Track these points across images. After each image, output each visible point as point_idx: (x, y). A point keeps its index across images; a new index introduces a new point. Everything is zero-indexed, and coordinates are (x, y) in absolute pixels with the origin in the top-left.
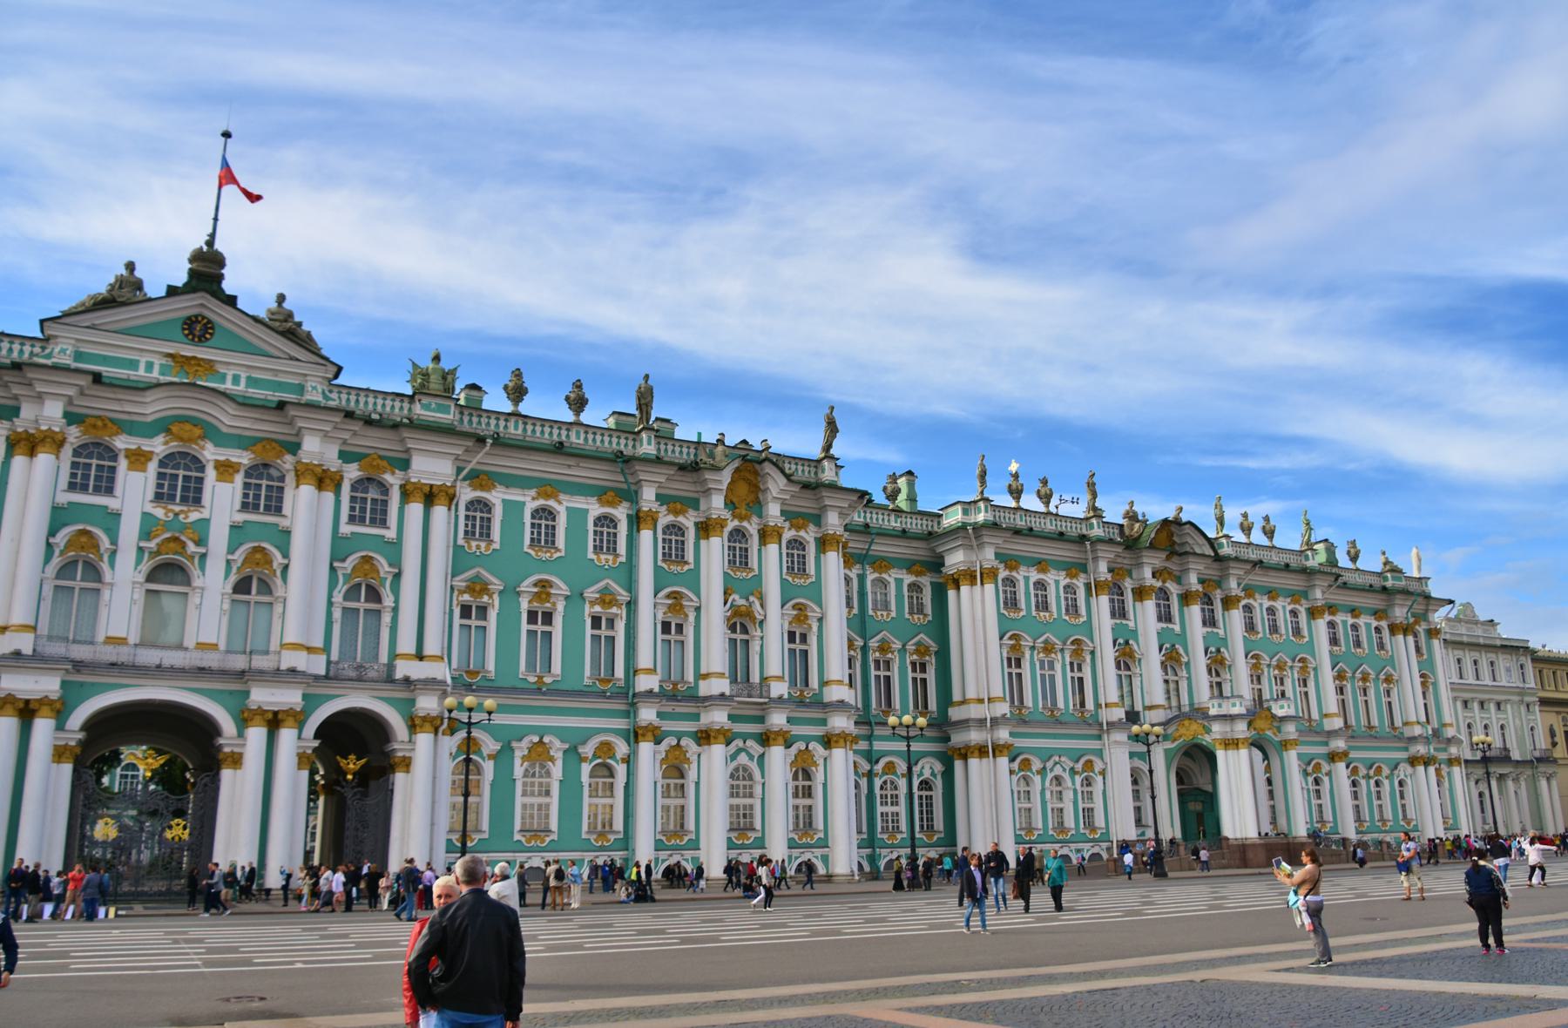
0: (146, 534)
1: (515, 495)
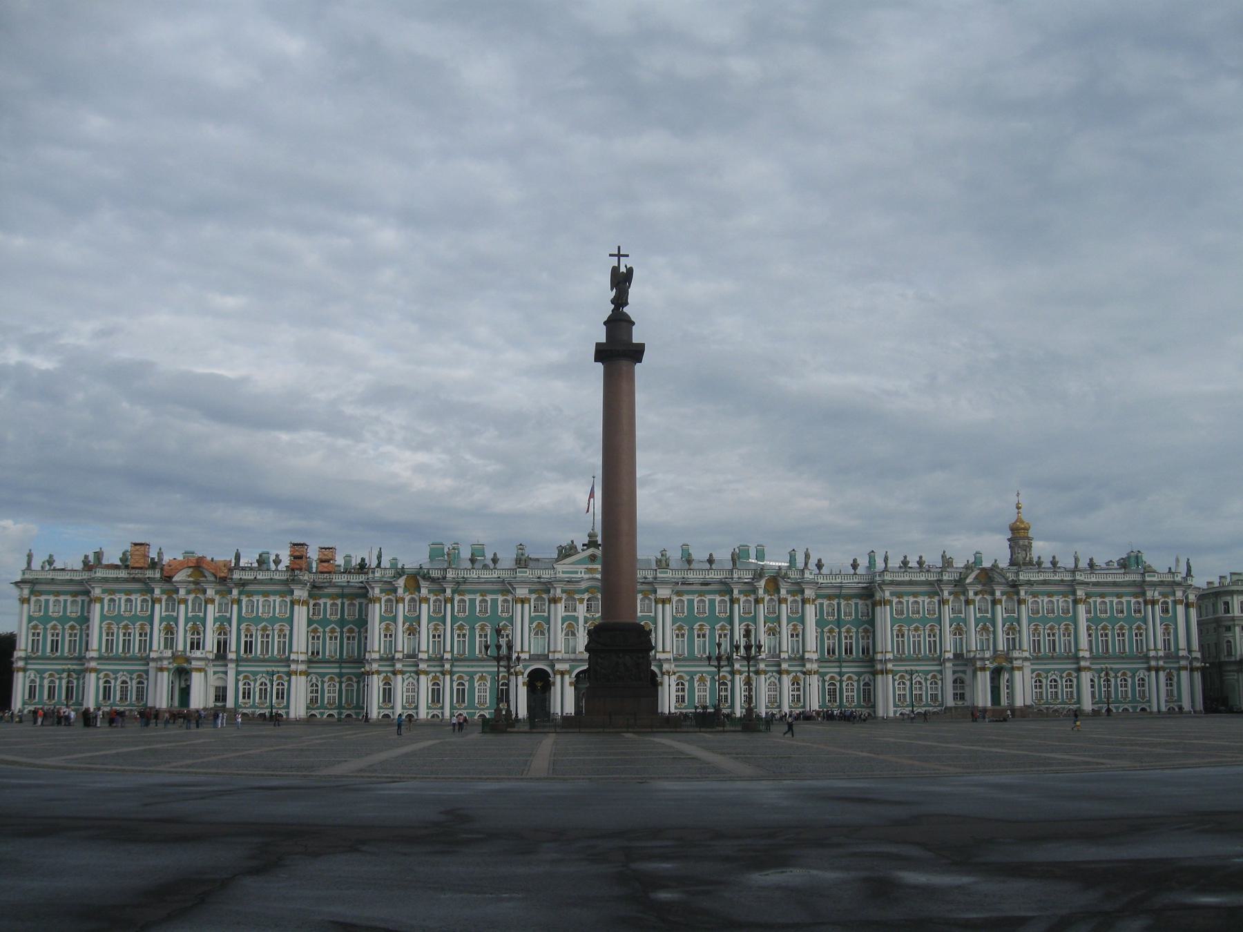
0: (586, 622)
1: (690, 597)
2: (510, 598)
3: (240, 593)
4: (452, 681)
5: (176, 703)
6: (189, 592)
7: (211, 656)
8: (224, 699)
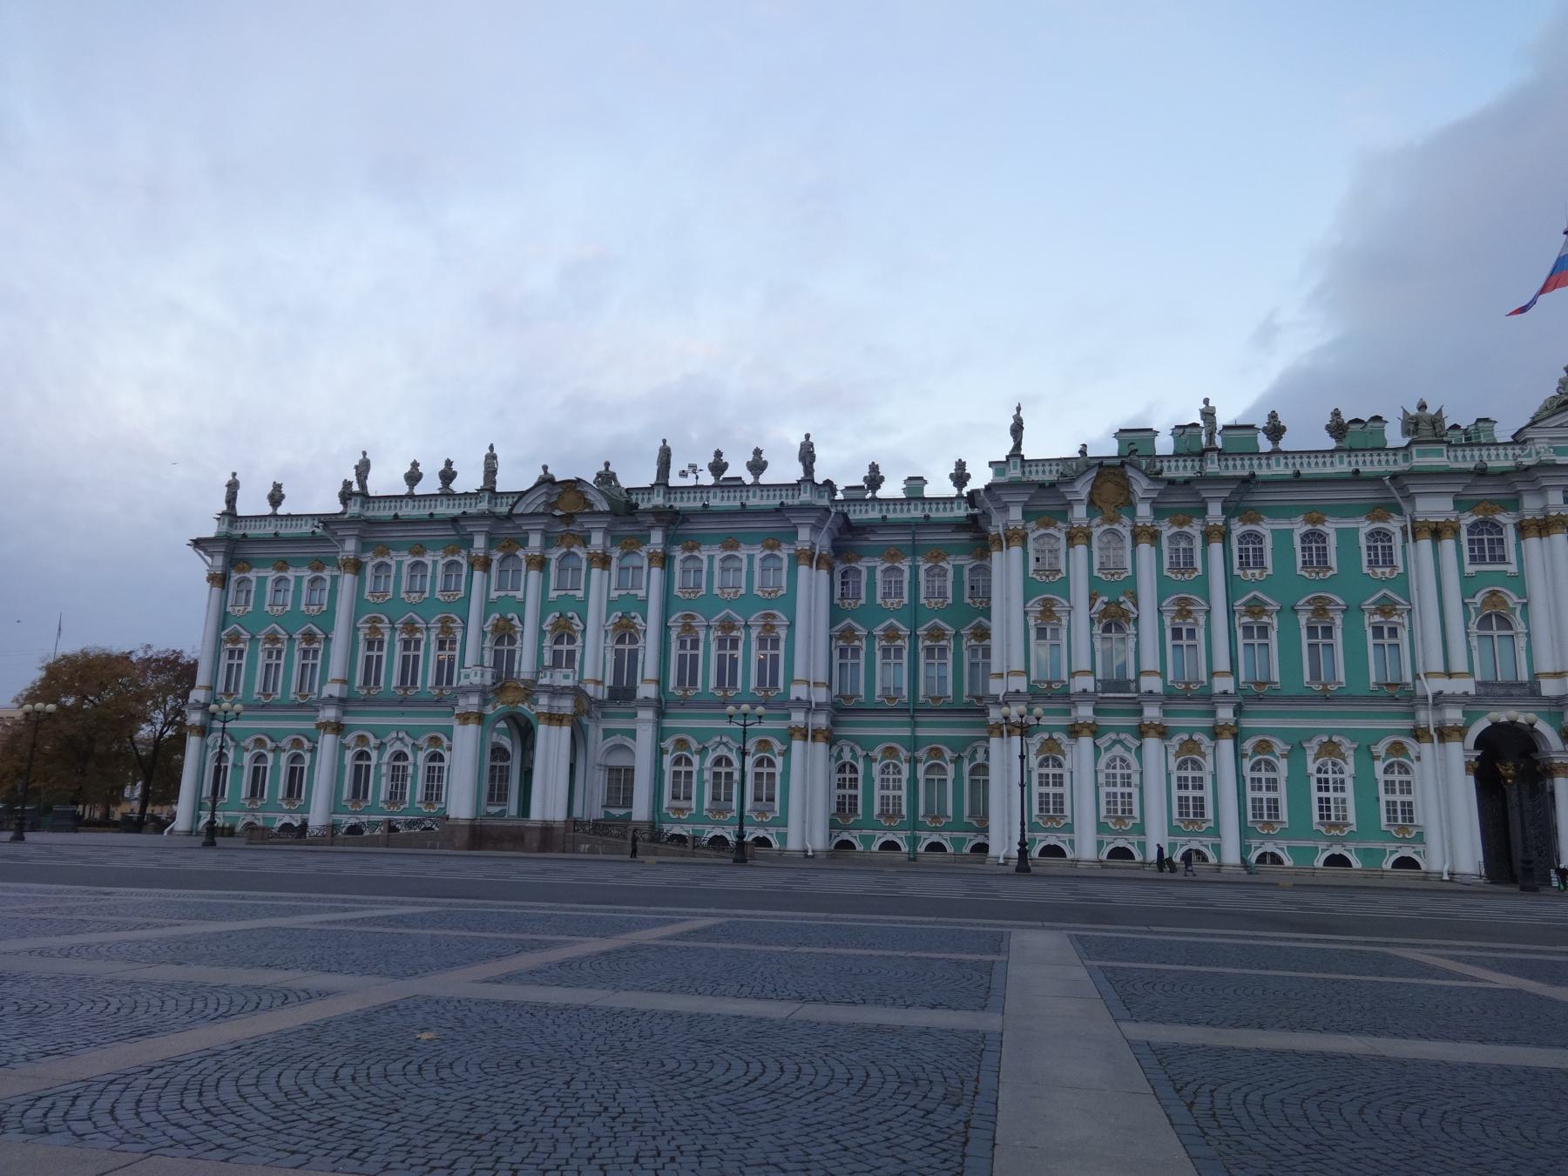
2: (1394, 525)
3: (670, 540)
4: (1239, 755)
5: (513, 807)
6: (549, 541)
7: (601, 693)
8: (628, 802)
